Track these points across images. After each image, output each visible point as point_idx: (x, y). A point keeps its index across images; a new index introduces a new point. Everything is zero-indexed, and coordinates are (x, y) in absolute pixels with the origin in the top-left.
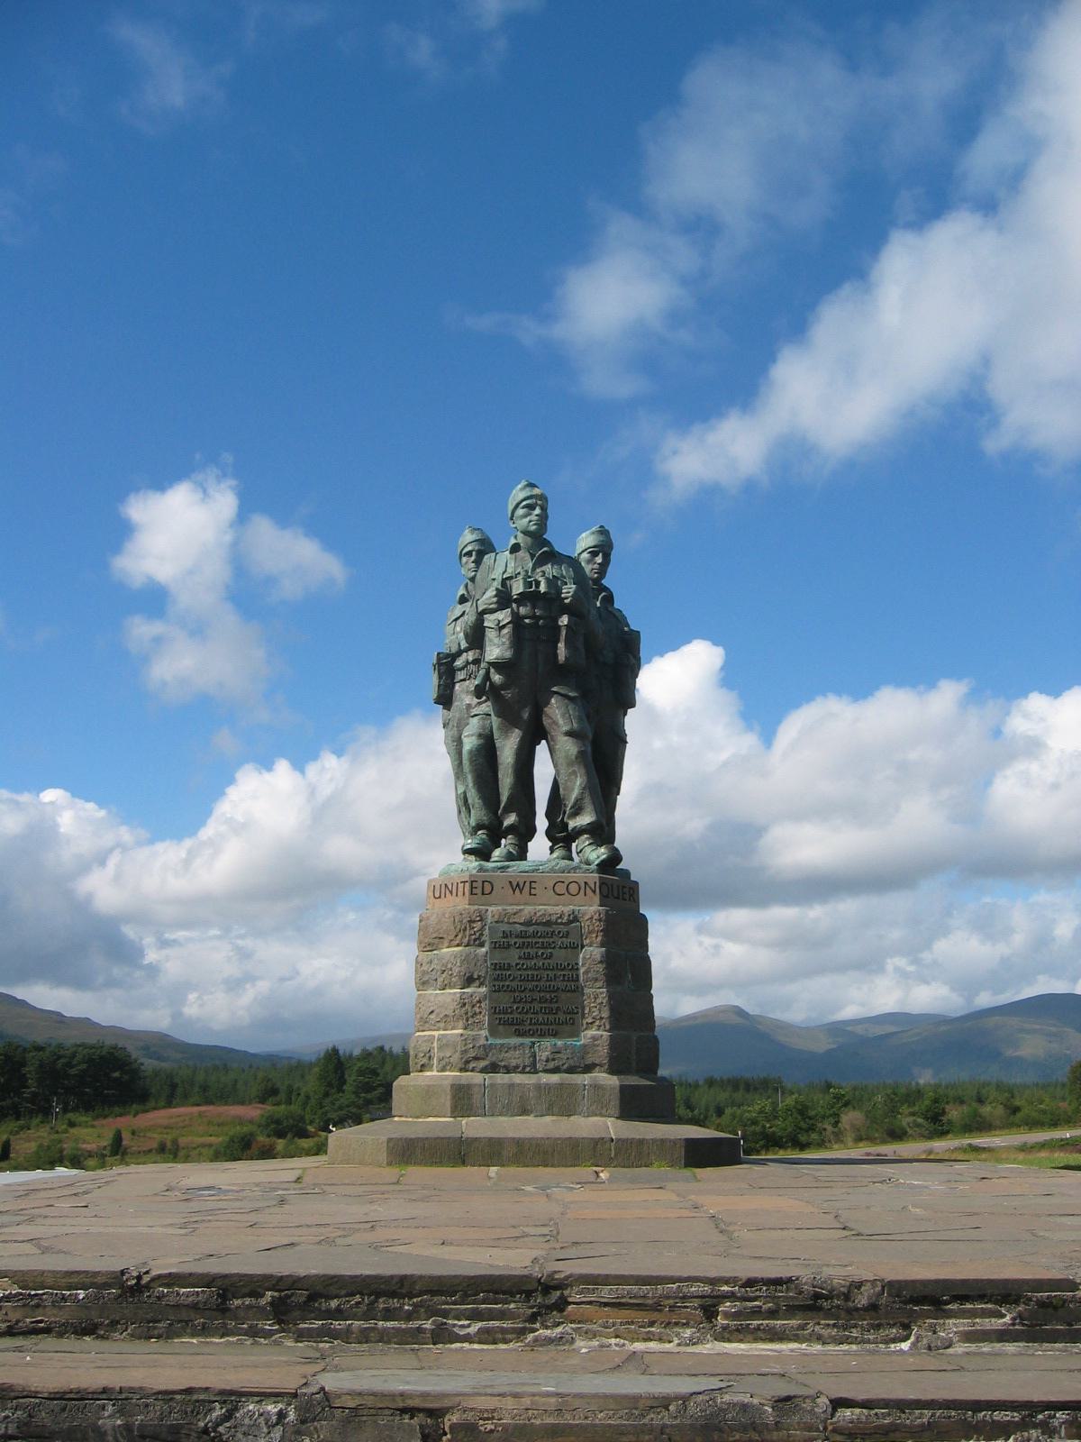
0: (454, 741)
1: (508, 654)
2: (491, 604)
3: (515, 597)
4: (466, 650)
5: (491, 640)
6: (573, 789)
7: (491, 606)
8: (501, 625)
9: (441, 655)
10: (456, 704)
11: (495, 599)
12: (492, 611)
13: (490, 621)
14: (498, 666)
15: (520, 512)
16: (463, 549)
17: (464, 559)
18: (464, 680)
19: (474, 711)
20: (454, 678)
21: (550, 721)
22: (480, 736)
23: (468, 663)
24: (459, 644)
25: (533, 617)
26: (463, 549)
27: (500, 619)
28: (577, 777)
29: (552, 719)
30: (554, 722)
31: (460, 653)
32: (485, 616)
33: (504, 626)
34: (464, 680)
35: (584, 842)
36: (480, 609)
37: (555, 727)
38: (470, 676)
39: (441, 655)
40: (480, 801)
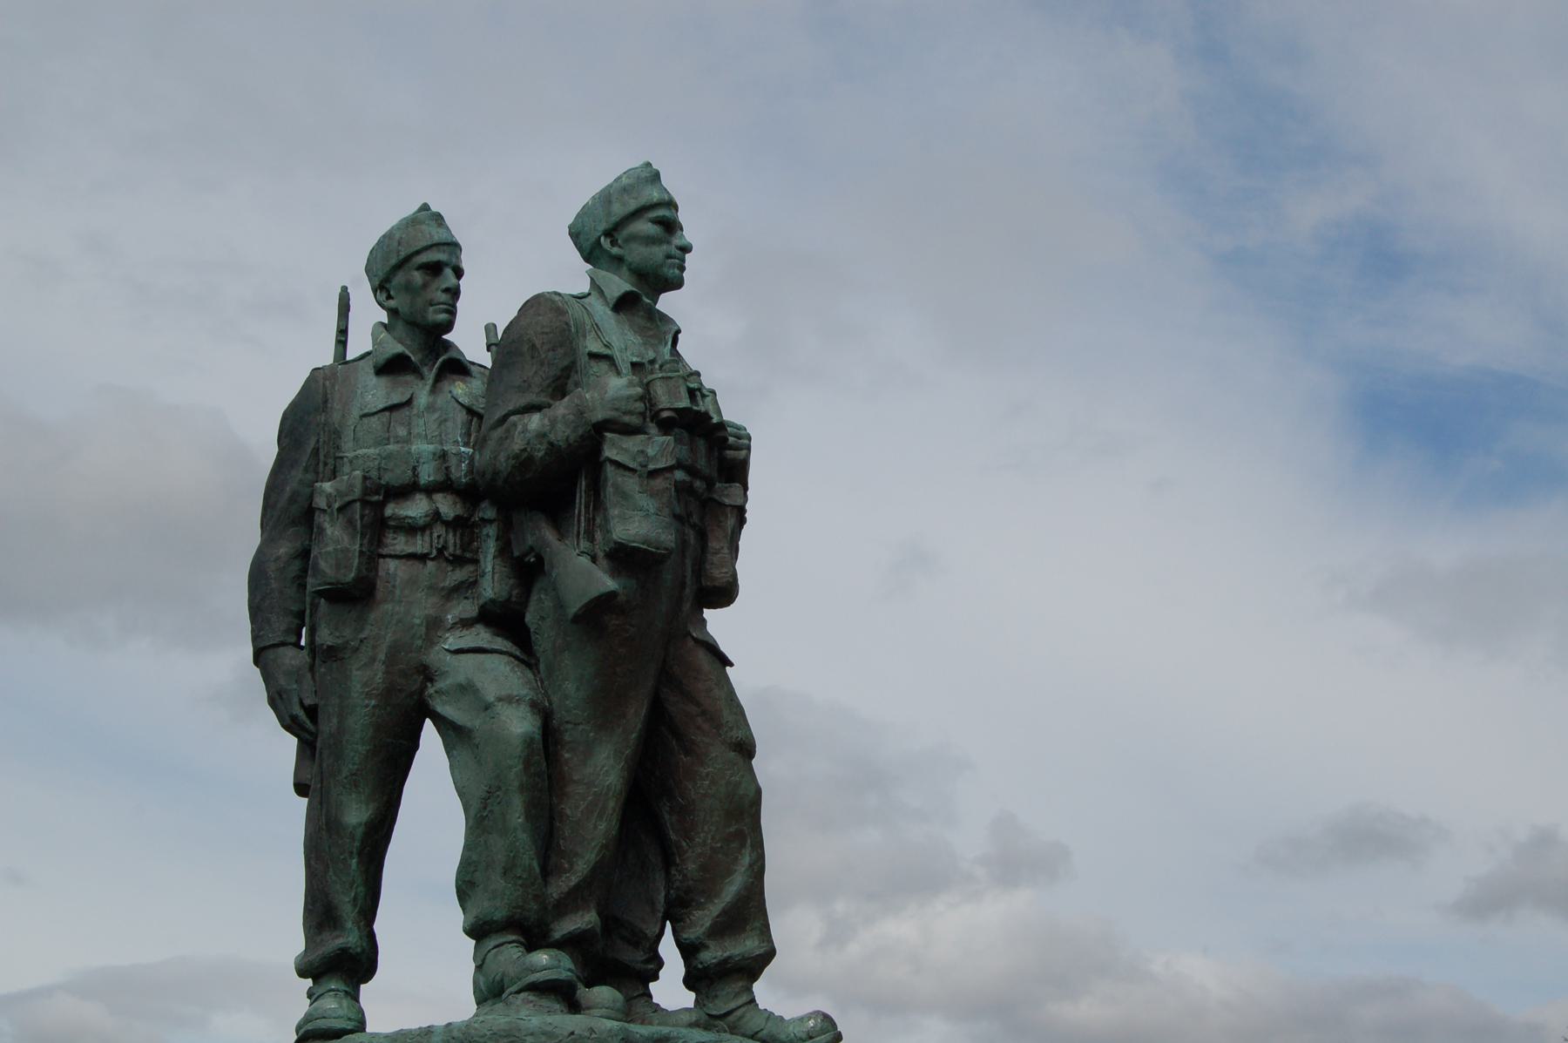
0: (368, 695)
1: (668, 538)
2: (630, 413)
3: (665, 414)
4: (430, 490)
5: (624, 496)
6: (730, 873)
7: (627, 419)
8: (651, 467)
9: (368, 483)
10: (385, 609)
11: (640, 406)
12: (629, 431)
13: (615, 449)
14: (623, 558)
15: (644, 227)
16: (418, 252)
17: (418, 277)
18: (422, 558)
19: (452, 641)
20: (380, 543)
21: (693, 709)
22: (534, 705)
23: (436, 516)
24: (414, 469)
25: (692, 471)
26: (418, 252)
27: (651, 452)
28: (743, 845)
29: (698, 704)
30: (704, 713)
31: (405, 491)
32: (608, 435)
33: (653, 474)
34: (422, 558)
35: (737, 995)
36: (599, 415)
37: (706, 726)
38: (440, 551)
39: (368, 483)
40: (535, 864)
